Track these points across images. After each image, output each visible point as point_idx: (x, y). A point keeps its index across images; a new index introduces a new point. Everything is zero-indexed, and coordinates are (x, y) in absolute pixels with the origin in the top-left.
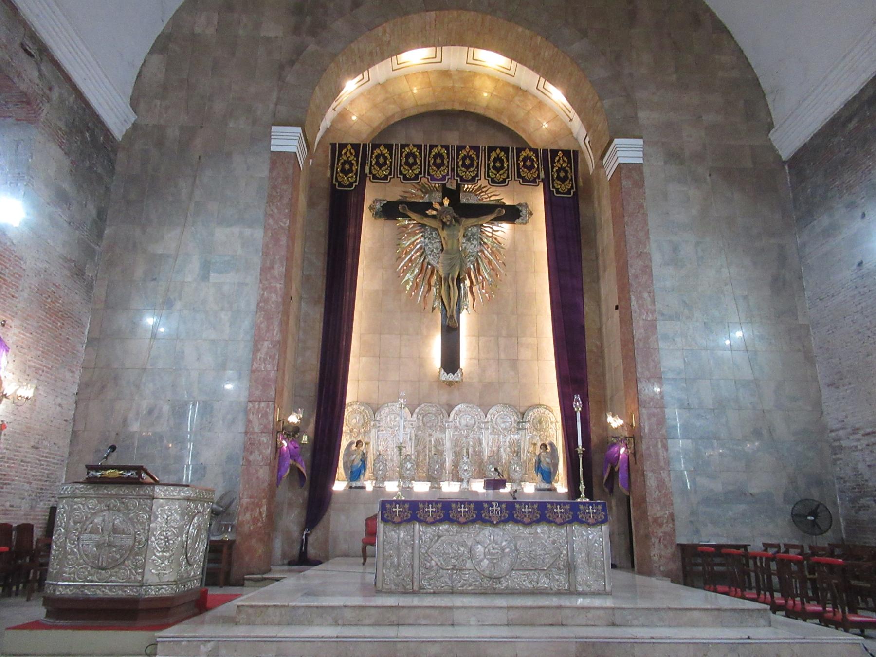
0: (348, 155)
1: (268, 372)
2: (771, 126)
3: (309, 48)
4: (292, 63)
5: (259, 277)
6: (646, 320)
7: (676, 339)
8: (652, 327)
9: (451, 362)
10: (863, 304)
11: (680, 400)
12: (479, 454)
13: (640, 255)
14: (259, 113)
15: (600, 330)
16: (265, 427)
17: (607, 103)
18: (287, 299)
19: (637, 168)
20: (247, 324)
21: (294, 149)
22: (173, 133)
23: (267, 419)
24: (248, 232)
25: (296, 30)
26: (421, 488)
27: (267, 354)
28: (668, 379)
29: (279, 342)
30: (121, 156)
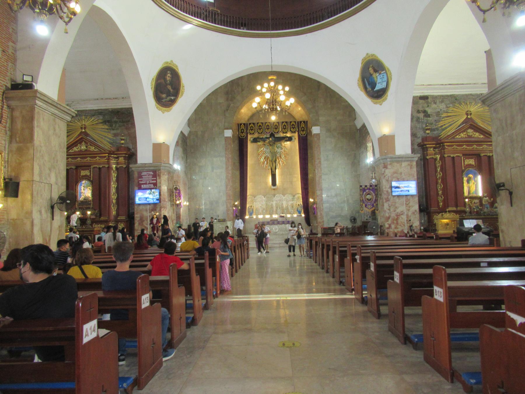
0: (243, 127)
2: (355, 119)
4: (227, 110)
8: (320, 177)
9: (274, 183)
12: (283, 207)
13: (318, 159)
19: (318, 135)
22: (200, 133)
24: (221, 159)
25: (227, 100)
26: (268, 216)
30: (188, 140)
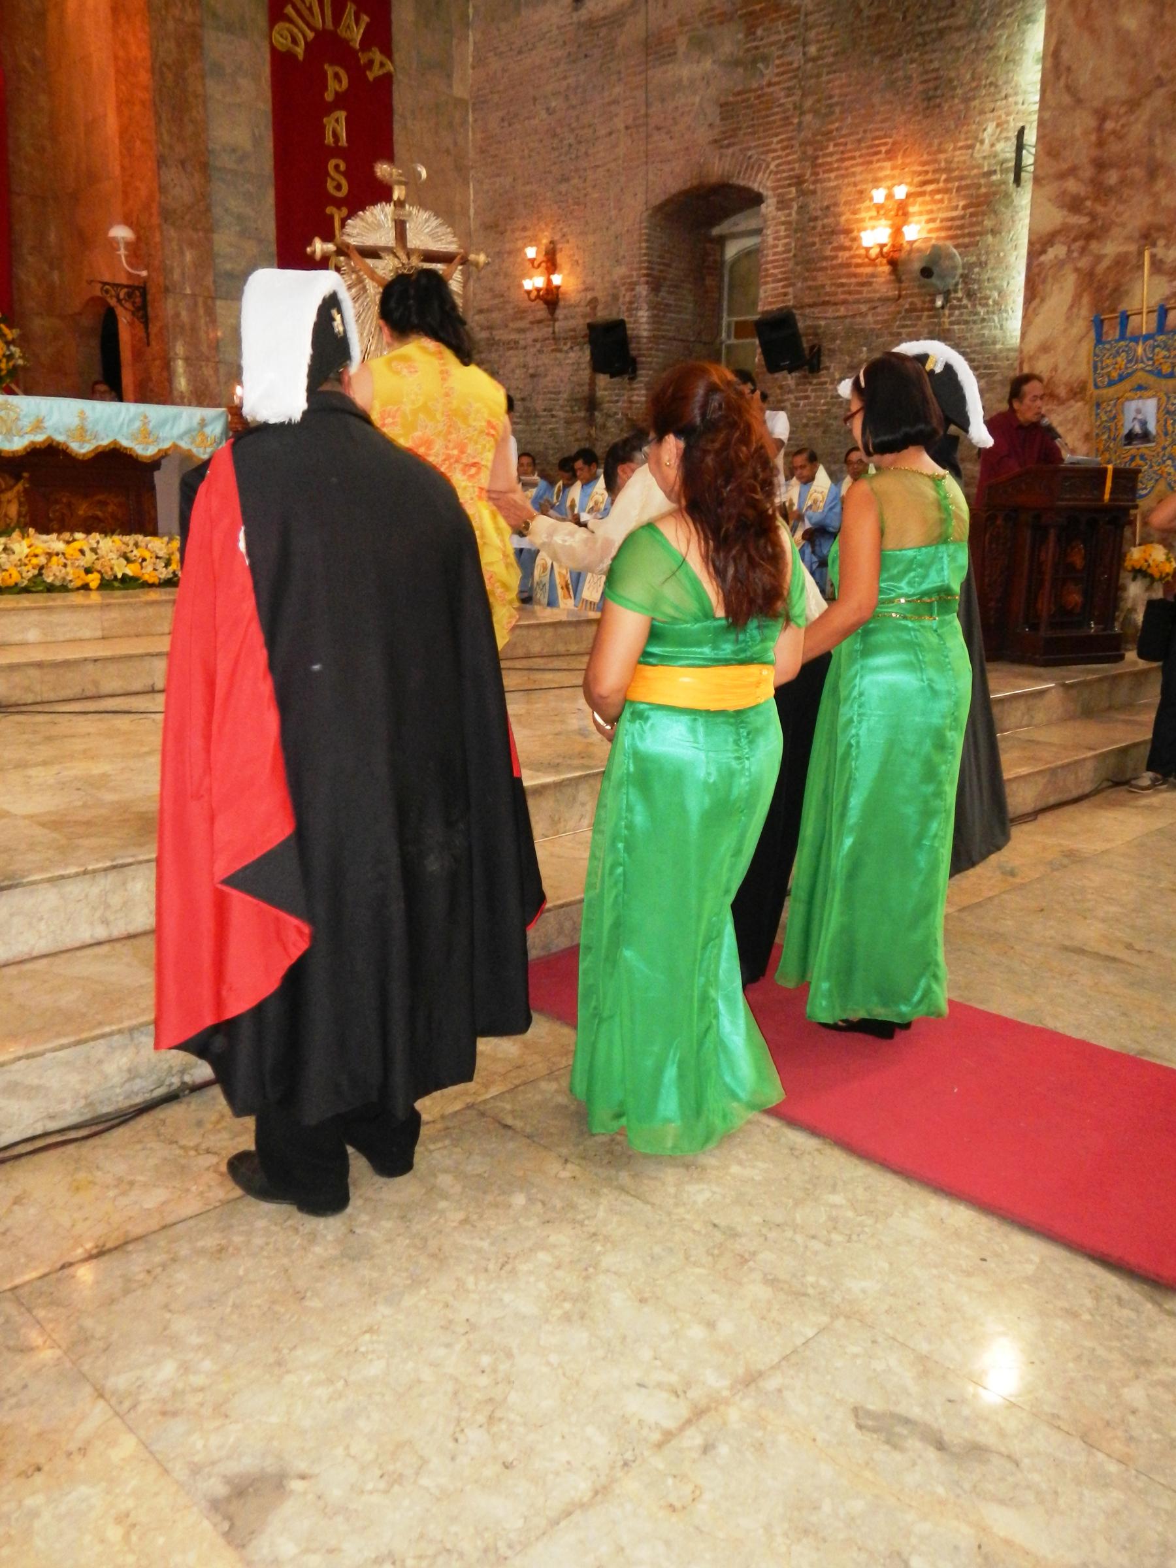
6: (181, 20)
7: (243, 82)
8: (192, 40)
10: (570, 81)
11: (240, 218)
15: (41, 15)
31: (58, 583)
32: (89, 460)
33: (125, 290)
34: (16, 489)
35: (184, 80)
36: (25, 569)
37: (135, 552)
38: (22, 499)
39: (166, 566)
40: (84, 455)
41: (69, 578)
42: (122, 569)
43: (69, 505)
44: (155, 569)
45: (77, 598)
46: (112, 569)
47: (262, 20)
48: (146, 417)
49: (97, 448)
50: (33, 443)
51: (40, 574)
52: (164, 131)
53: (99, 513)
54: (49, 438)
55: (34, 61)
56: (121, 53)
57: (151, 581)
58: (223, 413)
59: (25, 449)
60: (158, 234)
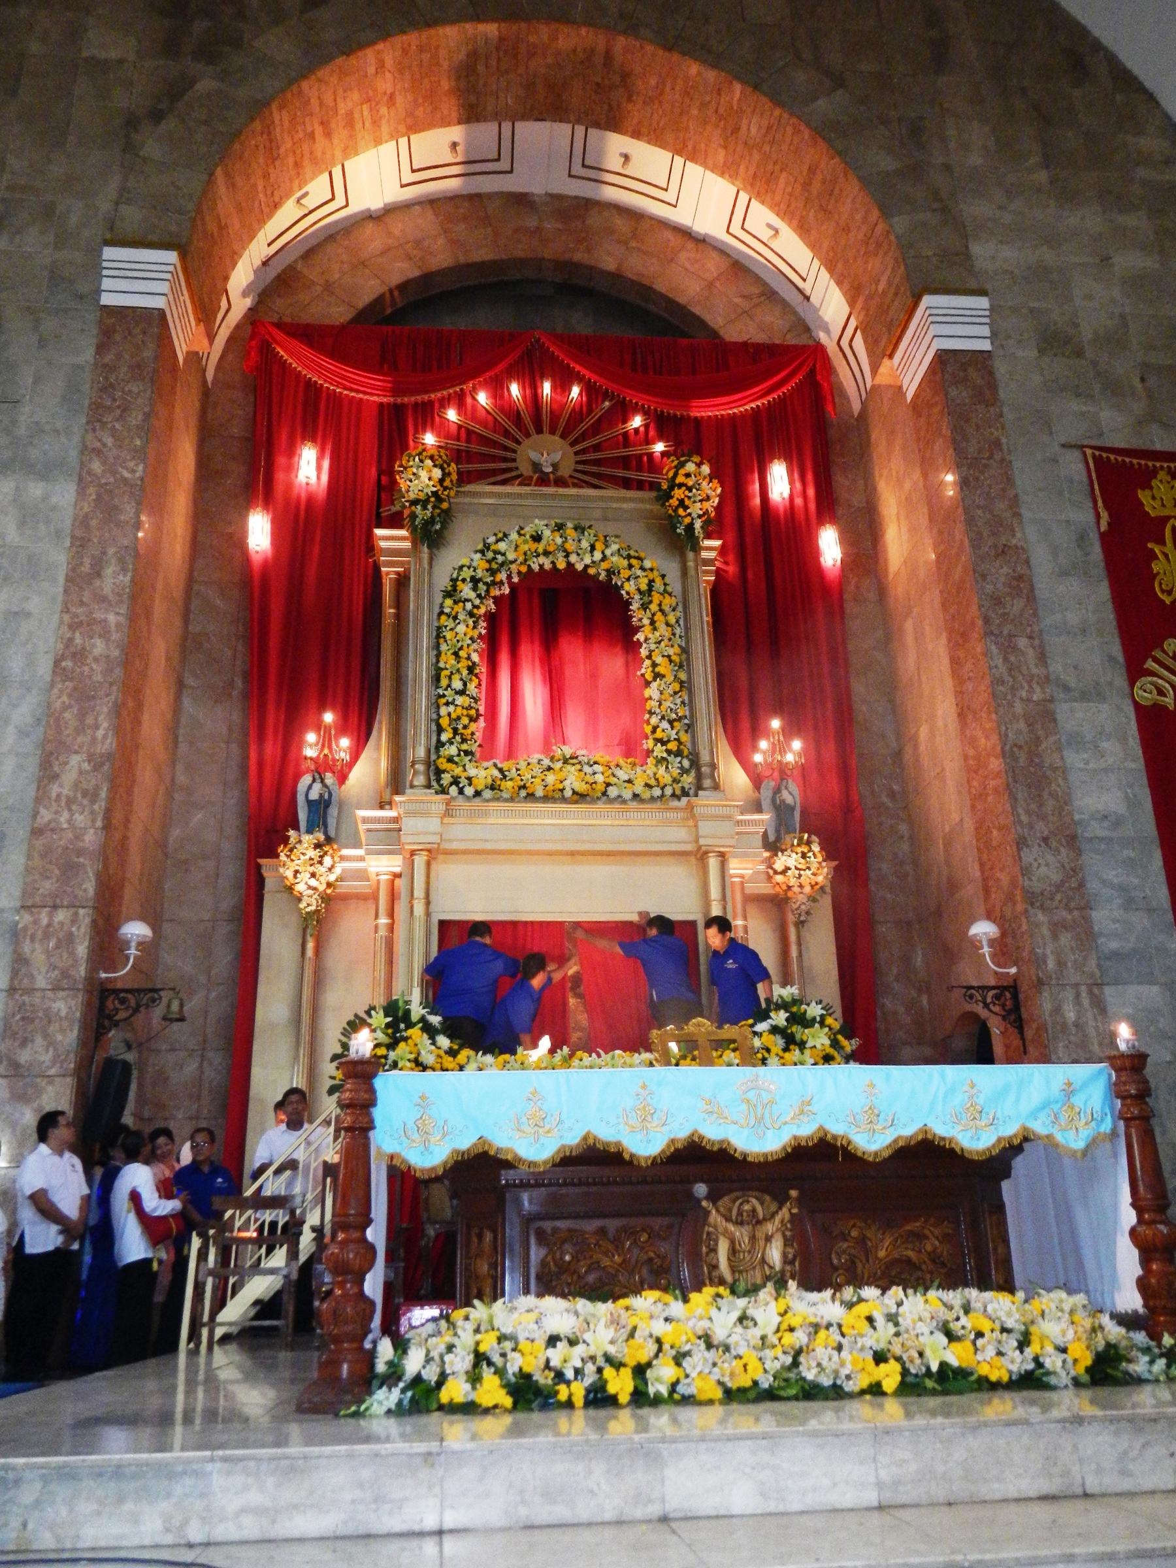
1: (78, 838)
3: (198, 86)
5: (60, 598)
6: (1029, 700)
8: (1044, 716)
11: (1122, 889)
13: (1003, 551)
14: (74, 219)
15: (898, 755)
16: (65, 974)
17: (901, 223)
18: (133, 653)
20: (24, 712)
21: (159, 303)
23: (72, 953)
24: (36, 490)
27: (76, 785)
28: (1091, 840)
29: (109, 756)
31: (826, 1381)
32: (885, 1160)
33: (991, 993)
34: (778, 1218)
35: (1039, 756)
36: (769, 1353)
37: (964, 1320)
38: (788, 1233)
39: (1023, 1345)
40: (876, 1154)
41: (844, 1372)
42: (941, 1352)
43: (862, 1241)
44: (1000, 1354)
45: (863, 1409)
46: (921, 1354)
47: (1121, 681)
48: (973, 1086)
49: (896, 1141)
50: (795, 1138)
51: (796, 1364)
52: (1020, 811)
53: (910, 1253)
54: (821, 1128)
55: (892, 794)
56: (971, 752)
57: (993, 1378)
58: (1100, 1072)
59: (784, 1148)
60: (1024, 920)
